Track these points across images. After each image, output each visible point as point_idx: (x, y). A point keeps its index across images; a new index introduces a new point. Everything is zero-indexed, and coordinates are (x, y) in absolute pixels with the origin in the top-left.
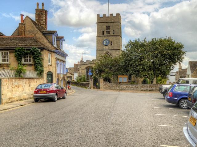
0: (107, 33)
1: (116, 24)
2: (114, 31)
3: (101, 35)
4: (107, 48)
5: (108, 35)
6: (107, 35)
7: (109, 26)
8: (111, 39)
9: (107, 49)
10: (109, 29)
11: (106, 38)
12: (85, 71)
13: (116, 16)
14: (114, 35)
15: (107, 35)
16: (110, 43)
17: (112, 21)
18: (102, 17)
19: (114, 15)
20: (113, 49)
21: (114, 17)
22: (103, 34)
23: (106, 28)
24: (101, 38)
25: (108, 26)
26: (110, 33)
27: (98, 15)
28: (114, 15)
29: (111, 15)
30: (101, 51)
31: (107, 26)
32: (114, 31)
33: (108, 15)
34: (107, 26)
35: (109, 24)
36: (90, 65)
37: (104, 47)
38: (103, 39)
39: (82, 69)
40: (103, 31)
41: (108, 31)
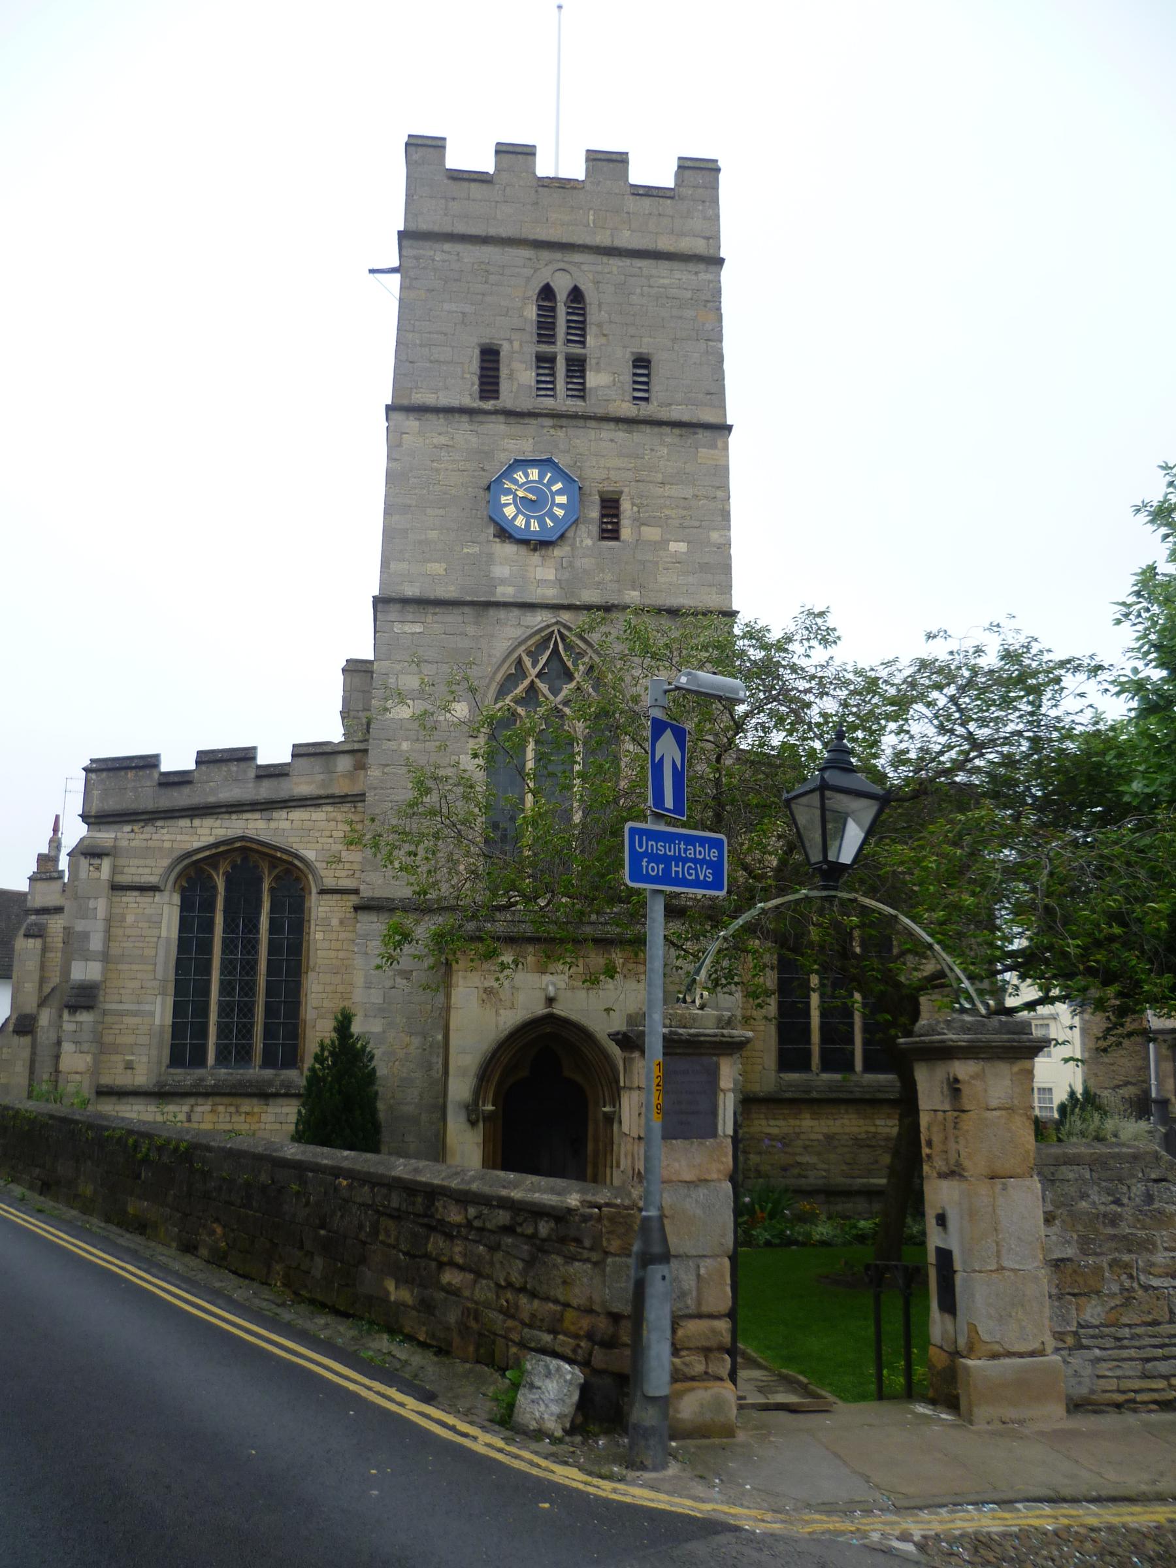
0: (545, 386)
1: (666, 276)
3: (464, 392)
4: (542, 576)
5: (562, 402)
6: (548, 403)
7: (576, 295)
8: (604, 457)
9: (550, 594)
10: (579, 328)
12: (166, 913)
13: (666, 180)
14: (646, 410)
15: (548, 403)
16: (595, 514)
17: (626, 239)
18: (480, 178)
19: (638, 175)
21: (649, 192)
22: (489, 384)
23: (532, 312)
24: (463, 433)
25: (562, 296)
26: (593, 379)
27: (424, 151)
28: (638, 175)
29: (609, 164)
30: (453, 618)
31: (547, 292)
32: (642, 362)
33: (560, 160)
34: (547, 292)
35: (584, 273)
36: (254, 826)
37: (501, 571)
39: (116, 887)
40: (490, 356)
41: (560, 349)
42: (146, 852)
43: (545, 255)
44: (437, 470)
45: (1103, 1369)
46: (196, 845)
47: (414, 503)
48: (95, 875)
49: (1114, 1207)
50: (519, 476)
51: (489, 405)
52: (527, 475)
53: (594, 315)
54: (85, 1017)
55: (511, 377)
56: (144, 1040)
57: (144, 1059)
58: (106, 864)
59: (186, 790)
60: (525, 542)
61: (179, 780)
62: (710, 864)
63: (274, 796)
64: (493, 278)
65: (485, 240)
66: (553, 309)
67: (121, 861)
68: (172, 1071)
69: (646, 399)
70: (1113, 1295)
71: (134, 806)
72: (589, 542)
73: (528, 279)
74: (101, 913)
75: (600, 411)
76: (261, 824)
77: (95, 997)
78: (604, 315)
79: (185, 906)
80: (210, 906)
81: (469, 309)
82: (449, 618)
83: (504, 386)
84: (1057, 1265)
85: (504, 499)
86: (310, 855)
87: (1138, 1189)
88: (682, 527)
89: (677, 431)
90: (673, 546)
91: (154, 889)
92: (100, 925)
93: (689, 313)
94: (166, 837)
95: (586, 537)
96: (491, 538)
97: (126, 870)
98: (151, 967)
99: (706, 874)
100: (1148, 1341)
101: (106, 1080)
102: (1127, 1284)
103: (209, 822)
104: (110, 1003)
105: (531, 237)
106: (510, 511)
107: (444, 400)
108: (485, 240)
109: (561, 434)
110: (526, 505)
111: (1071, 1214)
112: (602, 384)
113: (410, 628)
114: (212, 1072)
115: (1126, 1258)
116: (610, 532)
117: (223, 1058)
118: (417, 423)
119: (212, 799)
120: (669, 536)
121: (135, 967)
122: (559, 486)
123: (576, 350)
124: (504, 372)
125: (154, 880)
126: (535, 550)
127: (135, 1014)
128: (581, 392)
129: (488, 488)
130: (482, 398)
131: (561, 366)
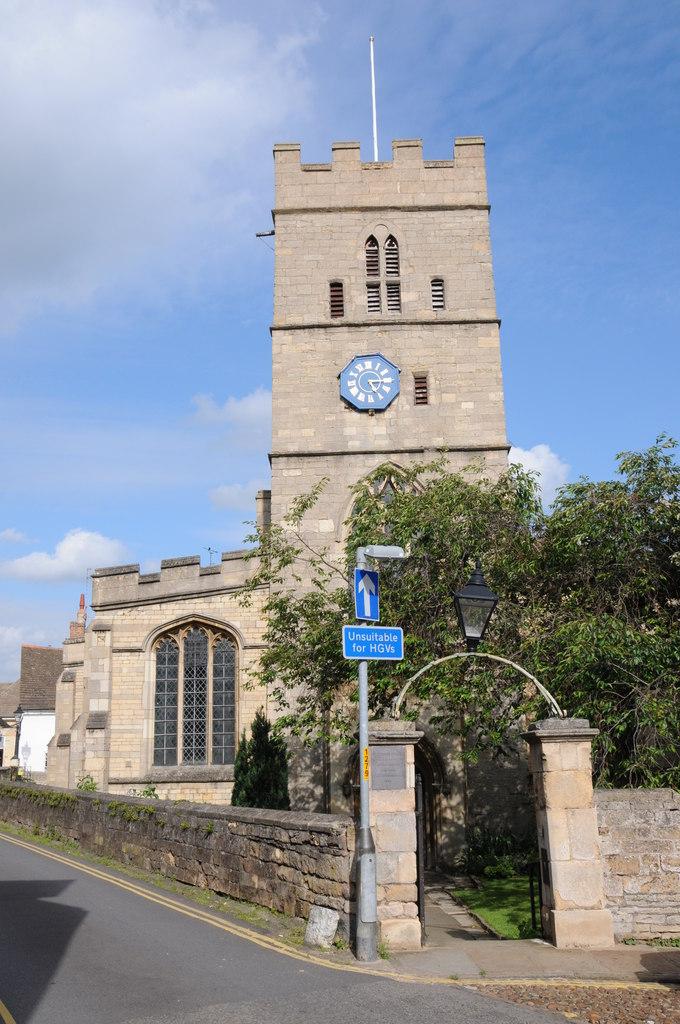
0: (375, 305)
2: (437, 282)
3: (321, 313)
4: (375, 432)
5: (386, 314)
6: (376, 316)
8: (415, 349)
9: (385, 445)
10: (394, 264)
11: (363, 348)
12: (148, 663)
14: (442, 315)
16: (410, 387)
20: (439, 442)
22: (337, 307)
23: (362, 256)
26: (405, 297)
31: (372, 240)
32: (437, 282)
35: (396, 224)
37: (349, 431)
38: (338, 354)
40: (336, 287)
41: (383, 278)
42: (132, 628)
43: (369, 215)
44: (306, 367)
45: (640, 918)
46: (165, 621)
47: (291, 390)
48: (102, 643)
49: (645, 825)
50: (359, 367)
51: (337, 321)
52: (364, 366)
53: (404, 254)
54: (99, 734)
55: (351, 301)
56: (138, 748)
57: (138, 761)
58: (108, 634)
59: (156, 585)
60: (366, 411)
61: (152, 580)
62: (393, 644)
63: (212, 588)
64: (335, 236)
65: (329, 210)
66: (377, 252)
67: (115, 634)
68: (156, 768)
69: (442, 307)
70: (644, 876)
71: (123, 598)
72: (407, 407)
73: (359, 234)
74: (107, 669)
75: (411, 318)
76: (205, 606)
77: (106, 721)
78: (411, 253)
79: (160, 660)
80: (174, 660)
81: (320, 257)
82: (320, 465)
83: (347, 307)
84: (611, 857)
85: (349, 384)
86: (237, 624)
87: (660, 815)
88: (470, 392)
89: (463, 326)
90: (464, 406)
91: (139, 650)
92: (106, 675)
93: (467, 246)
94: (146, 617)
95: (405, 402)
96: (343, 409)
97: (121, 639)
98: (138, 702)
99: (391, 649)
100: (667, 903)
101: (113, 775)
102: (654, 869)
103: (171, 606)
104: (114, 724)
105: (359, 205)
106: (354, 391)
107: (308, 321)
108: (329, 210)
109: (385, 336)
110: (364, 385)
111: (618, 829)
112: (411, 299)
113: (293, 473)
114: (181, 766)
115: (653, 854)
116: (422, 400)
117: (187, 755)
118: (290, 337)
119: (173, 591)
120: (460, 399)
121: (128, 702)
122: (386, 371)
123: (393, 278)
124: (346, 298)
125: (138, 645)
126: (372, 415)
127: (130, 731)
128: (397, 306)
129: (339, 377)
130: (333, 316)
131: (383, 289)
